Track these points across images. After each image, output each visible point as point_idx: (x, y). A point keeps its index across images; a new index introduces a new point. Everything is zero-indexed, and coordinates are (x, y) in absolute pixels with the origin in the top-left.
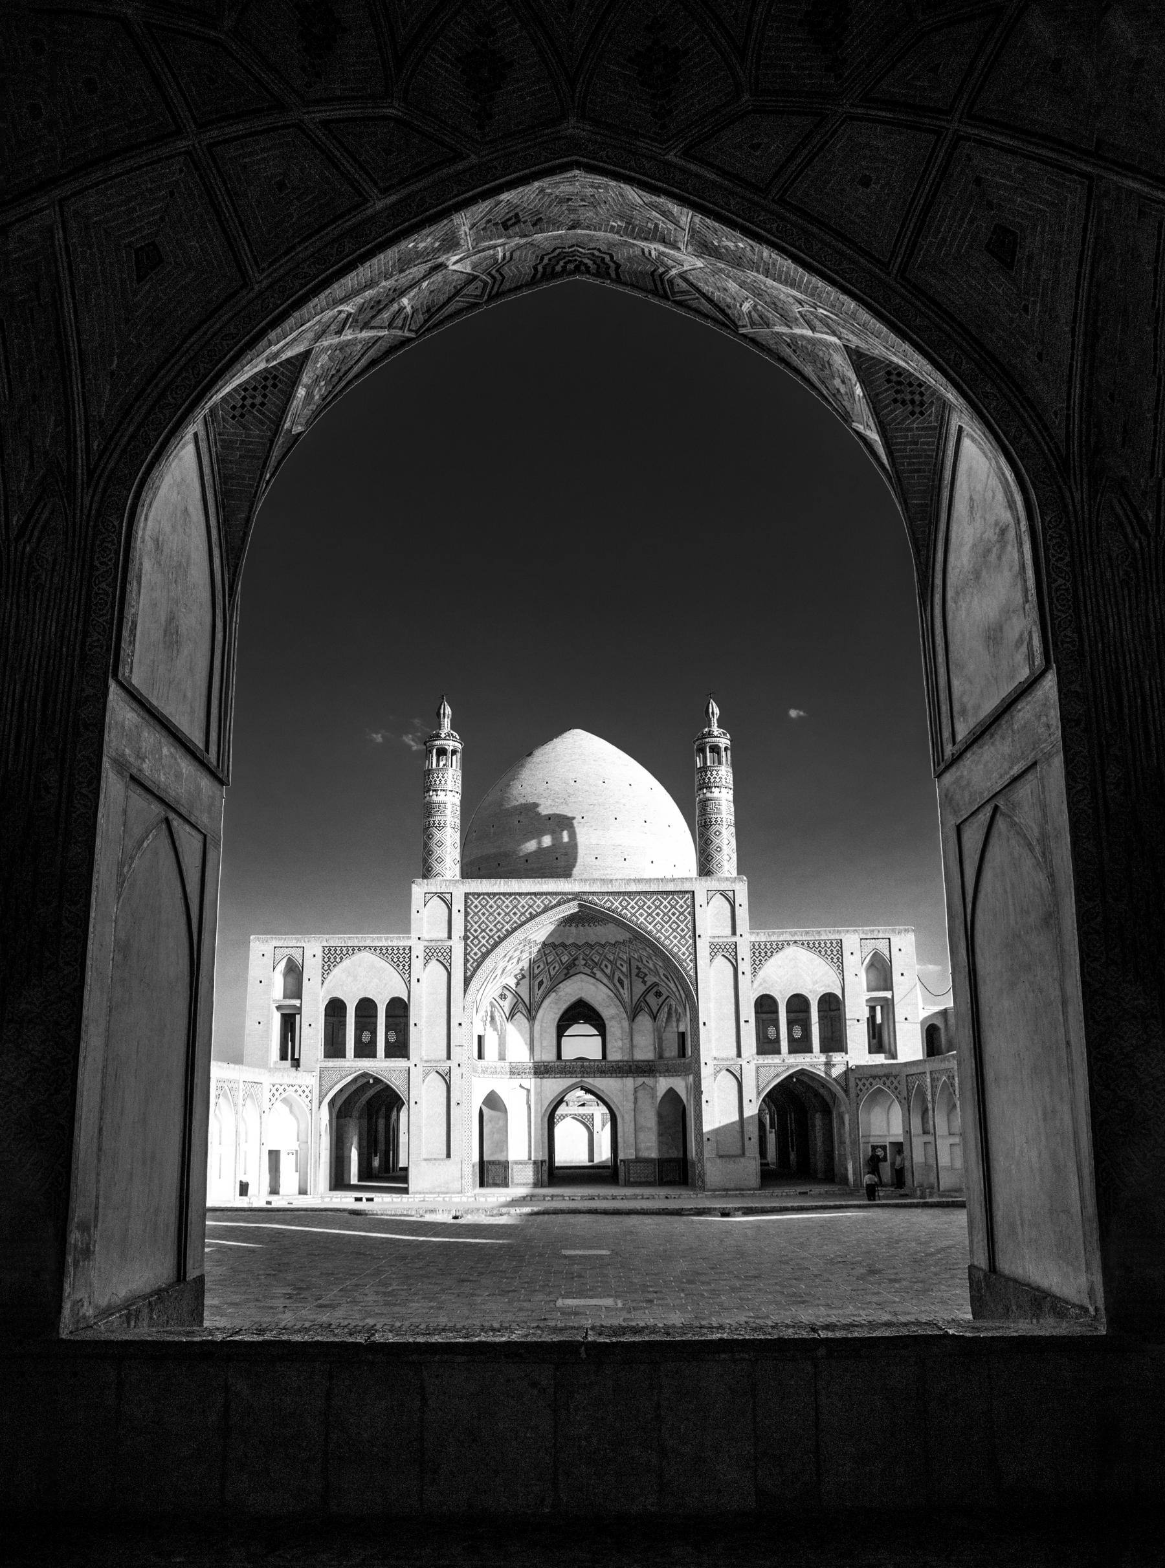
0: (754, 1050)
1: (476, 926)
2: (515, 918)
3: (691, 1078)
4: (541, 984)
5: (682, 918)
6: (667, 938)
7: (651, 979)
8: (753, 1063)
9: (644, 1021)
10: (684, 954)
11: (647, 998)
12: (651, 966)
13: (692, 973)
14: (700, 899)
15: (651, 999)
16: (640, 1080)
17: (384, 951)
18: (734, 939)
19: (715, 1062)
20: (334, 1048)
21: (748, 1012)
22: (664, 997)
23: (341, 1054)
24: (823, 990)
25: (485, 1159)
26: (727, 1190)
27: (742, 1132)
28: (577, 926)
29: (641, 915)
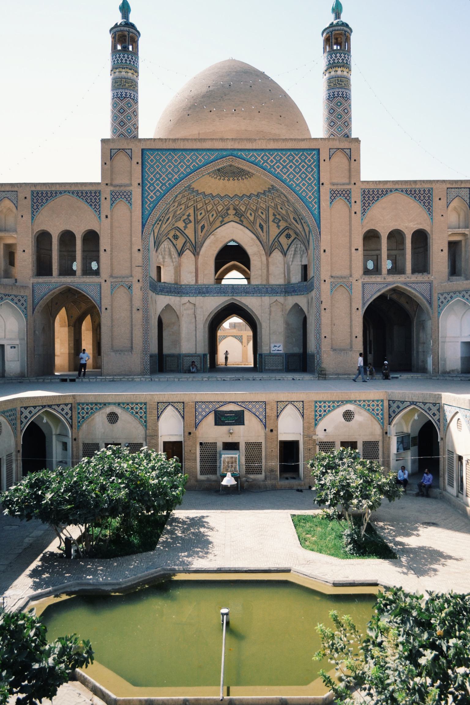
0: (361, 272)
1: (152, 176)
2: (182, 170)
3: (313, 293)
4: (203, 227)
5: (309, 170)
6: (298, 185)
7: (283, 225)
8: (360, 282)
9: (277, 255)
10: (310, 197)
11: (280, 239)
12: (284, 212)
13: (316, 212)
14: (324, 155)
15: (283, 240)
16: (275, 298)
17: (80, 194)
18: (348, 187)
19: (332, 280)
20: (43, 268)
21: (358, 242)
22: (292, 238)
23: (49, 273)
24: (415, 227)
25: (166, 351)
26: (338, 374)
27: (351, 332)
28: (229, 180)
29: (278, 167)
